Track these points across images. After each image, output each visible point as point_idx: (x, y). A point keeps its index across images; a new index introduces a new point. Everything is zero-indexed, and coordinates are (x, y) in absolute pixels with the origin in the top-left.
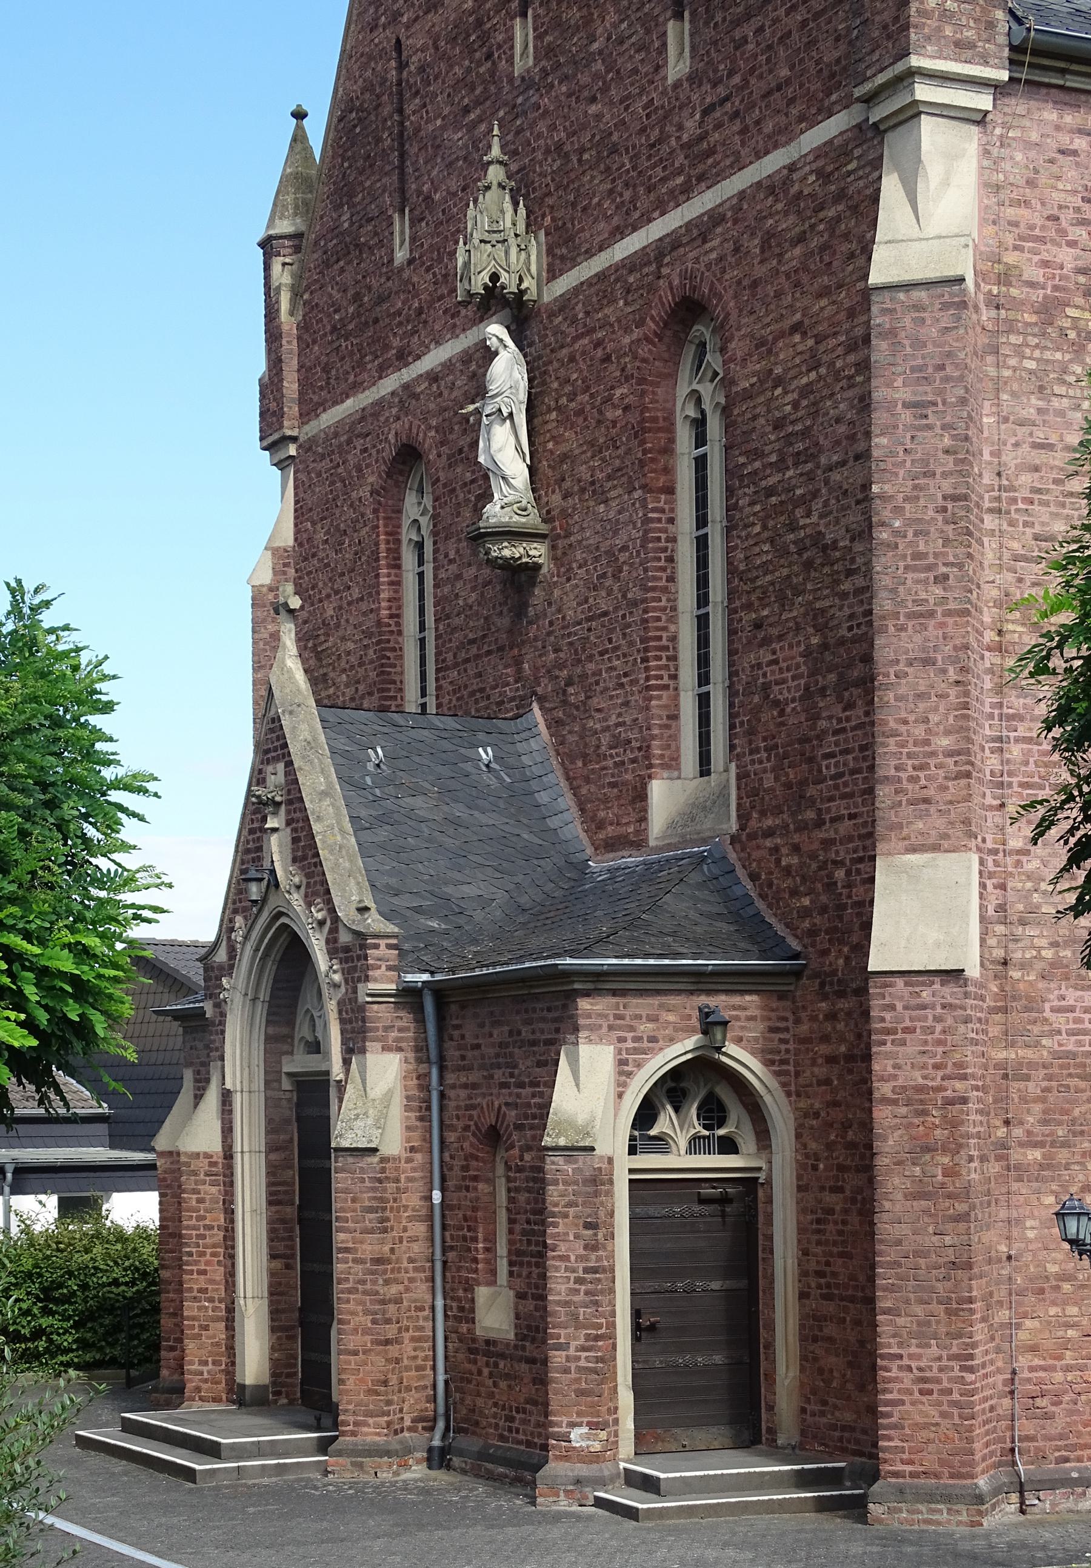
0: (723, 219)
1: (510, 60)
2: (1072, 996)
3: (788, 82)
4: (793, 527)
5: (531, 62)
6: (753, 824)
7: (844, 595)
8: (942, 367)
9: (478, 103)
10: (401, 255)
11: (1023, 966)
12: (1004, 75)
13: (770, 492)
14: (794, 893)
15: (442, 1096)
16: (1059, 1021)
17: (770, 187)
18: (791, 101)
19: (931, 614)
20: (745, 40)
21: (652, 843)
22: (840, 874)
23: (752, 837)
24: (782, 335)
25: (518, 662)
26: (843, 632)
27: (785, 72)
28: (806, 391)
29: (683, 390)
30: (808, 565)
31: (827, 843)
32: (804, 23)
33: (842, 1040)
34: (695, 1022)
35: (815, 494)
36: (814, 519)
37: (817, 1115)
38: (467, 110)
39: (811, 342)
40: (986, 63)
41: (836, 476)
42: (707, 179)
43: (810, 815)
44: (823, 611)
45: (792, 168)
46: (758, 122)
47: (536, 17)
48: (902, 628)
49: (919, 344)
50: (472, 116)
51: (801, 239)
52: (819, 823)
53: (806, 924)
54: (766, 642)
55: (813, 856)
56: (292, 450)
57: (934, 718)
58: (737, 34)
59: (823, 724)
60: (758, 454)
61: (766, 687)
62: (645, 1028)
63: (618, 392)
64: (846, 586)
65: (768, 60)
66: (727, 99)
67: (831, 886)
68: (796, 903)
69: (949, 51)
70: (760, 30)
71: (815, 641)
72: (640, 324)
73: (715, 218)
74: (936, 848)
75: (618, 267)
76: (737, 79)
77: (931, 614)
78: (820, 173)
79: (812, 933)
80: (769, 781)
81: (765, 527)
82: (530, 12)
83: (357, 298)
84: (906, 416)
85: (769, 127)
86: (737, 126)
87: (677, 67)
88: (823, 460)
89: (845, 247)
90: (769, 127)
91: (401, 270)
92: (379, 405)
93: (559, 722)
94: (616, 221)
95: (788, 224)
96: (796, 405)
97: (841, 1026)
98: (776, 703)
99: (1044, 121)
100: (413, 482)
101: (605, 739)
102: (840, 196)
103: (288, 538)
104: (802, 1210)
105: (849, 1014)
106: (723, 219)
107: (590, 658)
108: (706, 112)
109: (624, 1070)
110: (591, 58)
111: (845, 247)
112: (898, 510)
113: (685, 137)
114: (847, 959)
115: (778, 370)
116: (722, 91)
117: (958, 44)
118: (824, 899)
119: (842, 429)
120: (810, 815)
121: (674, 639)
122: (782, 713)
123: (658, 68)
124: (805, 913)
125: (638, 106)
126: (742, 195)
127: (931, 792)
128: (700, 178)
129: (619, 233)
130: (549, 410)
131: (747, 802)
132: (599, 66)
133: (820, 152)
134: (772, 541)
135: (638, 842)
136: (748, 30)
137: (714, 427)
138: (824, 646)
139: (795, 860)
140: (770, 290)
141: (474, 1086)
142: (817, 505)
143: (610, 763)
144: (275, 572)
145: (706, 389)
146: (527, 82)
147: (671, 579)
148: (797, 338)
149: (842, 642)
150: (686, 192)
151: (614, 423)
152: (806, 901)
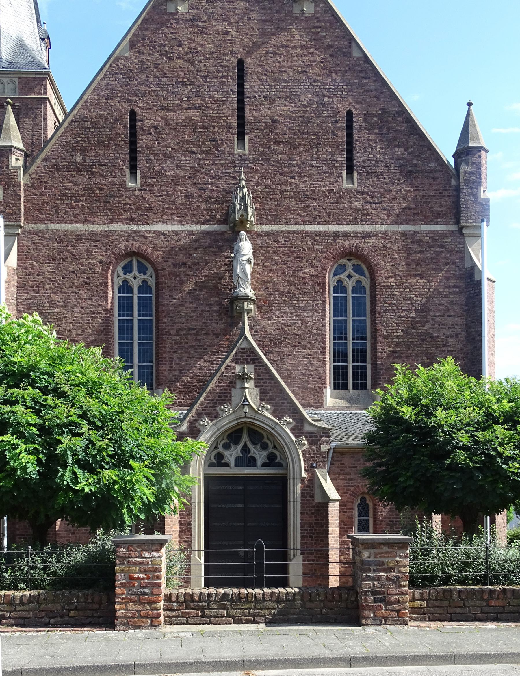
0: (376, 236)
3: (414, 208)
5: (247, 152)
9: (202, 152)
30: (423, 340)
32: (423, 196)
35: (427, 322)
36: (426, 328)
41: (438, 319)
44: (430, 354)
45: (416, 232)
47: (250, 139)
51: (420, 252)
56: (20, 231)
102: (442, 246)
119: (442, 308)
123: (336, 182)
128: (362, 220)
133: (430, 232)
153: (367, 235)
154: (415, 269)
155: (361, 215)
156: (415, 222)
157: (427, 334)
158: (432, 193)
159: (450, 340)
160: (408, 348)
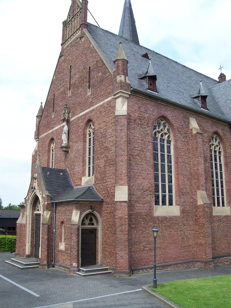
0: (94, 110)
1: (68, 95)
2: (138, 205)
3: (103, 94)
4: (103, 145)
6: (97, 182)
7: (110, 153)
8: (124, 125)
10: (53, 117)
11: (133, 201)
12: (130, 93)
13: (100, 141)
14: (102, 191)
15: (55, 217)
16: (137, 208)
17: (101, 106)
18: (104, 96)
19: (123, 155)
20: (98, 90)
21: (82, 185)
22: (109, 189)
23: (96, 184)
24: (102, 123)
25: (65, 163)
26: (110, 158)
27: (103, 93)
28: (105, 129)
29: (88, 130)
30: (105, 150)
31: (107, 185)
32: (106, 88)
33: (109, 210)
34: (90, 208)
35: (106, 141)
36: (106, 144)
37: (105, 220)
38: (62, 100)
39: (106, 123)
40: (128, 92)
41: (109, 139)
42: (92, 106)
43: (105, 181)
45: (104, 104)
46: (99, 99)
48: (119, 157)
49: (121, 122)
50: (63, 101)
51: (105, 111)
52: (106, 182)
53: (104, 195)
54: (99, 159)
55: (105, 186)
57: (123, 168)
58: (97, 89)
59: (106, 170)
60: (98, 137)
61: (99, 165)
62: (84, 208)
63: (80, 130)
64: (110, 152)
65: (101, 92)
66: (95, 97)
67: (107, 190)
68: (102, 192)
69: (125, 90)
70: (100, 89)
71: (106, 159)
72: (83, 122)
73: (93, 110)
74: (123, 185)
75: (81, 116)
76: (96, 95)
77: (123, 155)
78: (107, 104)
79: (105, 196)
80: (99, 177)
81: (99, 146)
82: (71, 90)
83: (47, 122)
84: (120, 131)
85: (101, 99)
86: (96, 99)
87: (89, 94)
88: (107, 137)
89: (111, 112)
90: (101, 99)
91: (53, 118)
92: (49, 134)
93: (70, 170)
94: (80, 111)
95: (103, 110)
96: (104, 131)
97: (109, 208)
98: (100, 167)
99: (134, 99)
100: (52, 142)
101: (76, 172)
103: (37, 149)
104: (102, 233)
105: (110, 207)
106: (94, 110)
107: (75, 162)
108: (92, 98)
109: (81, 214)
110: (78, 94)
111: (111, 112)
112: (119, 142)
113: (90, 101)
114: (110, 200)
115: (101, 127)
116: (95, 96)
117: (125, 89)
118: (106, 192)
119: (110, 133)
120: (105, 181)
121: (86, 160)
122: (101, 168)
124: (104, 194)
125: (84, 98)
126: (97, 107)
127: (122, 178)
128: (92, 106)
129: (81, 112)
130: (71, 133)
131: (96, 180)
132: (79, 94)
133: (107, 102)
134: (100, 147)
135: (80, 185)
136: (98, 89)
137: (92, 134)
138: (107, 160)
139: (102, 187)
140: (101, 118)
141: (60, 216)
142: (106, 143)
143: (77, 175)
144: (35, 153)
145: (91, 130)
146: (70, 97)
147: (86, 153)
148: (104, 123)
149: (110, 159)
150: (90, 107)
151: (79, 134)
152: (104, 192)
153: (91, 112)
154: (103, 120)
155: (92, 104)
156: (103, 100)
157: (106, 147)
158: (107, 86)
159: (112, 147)
160: (101, 155)
